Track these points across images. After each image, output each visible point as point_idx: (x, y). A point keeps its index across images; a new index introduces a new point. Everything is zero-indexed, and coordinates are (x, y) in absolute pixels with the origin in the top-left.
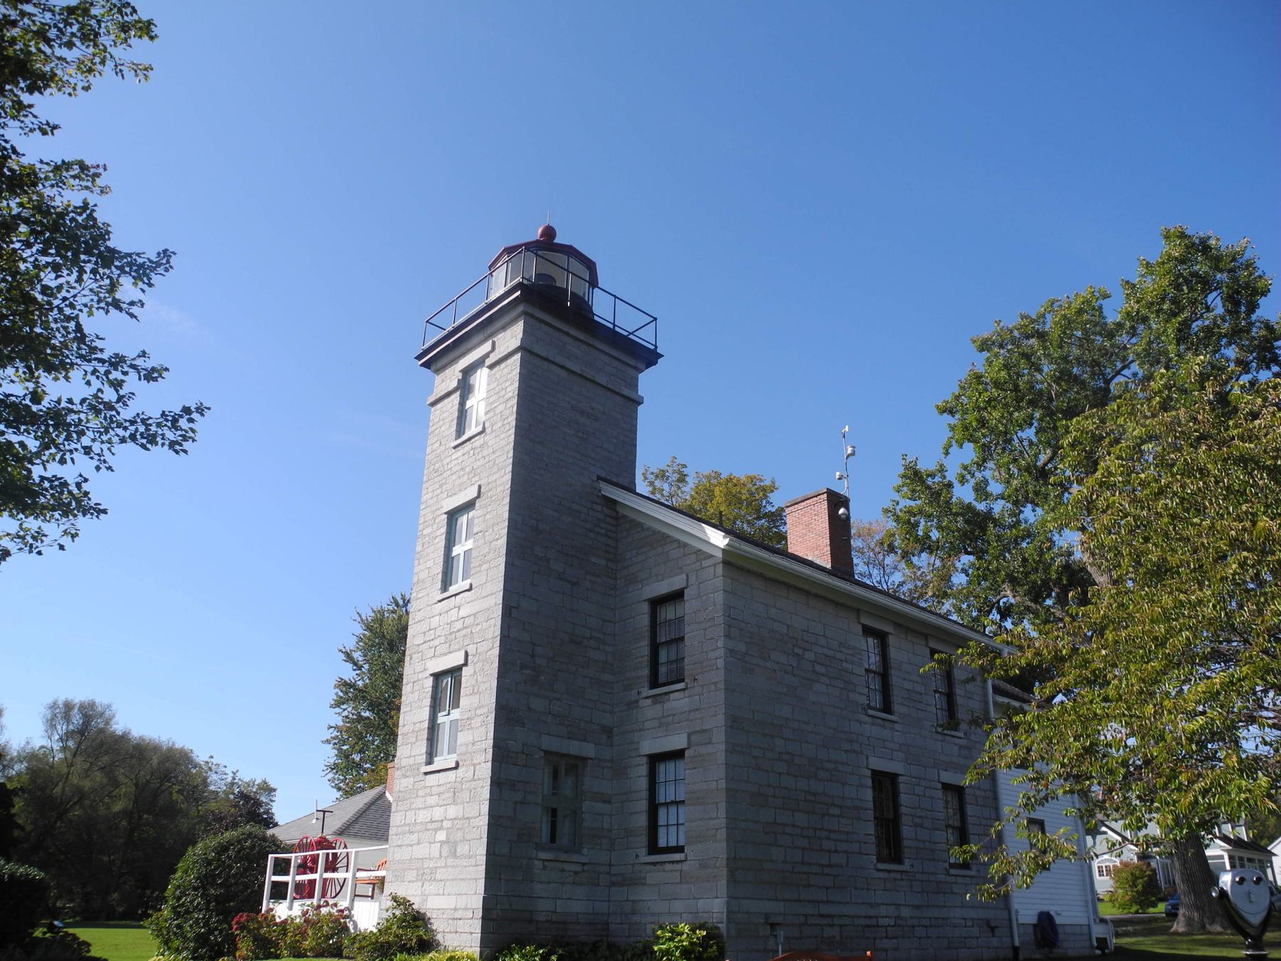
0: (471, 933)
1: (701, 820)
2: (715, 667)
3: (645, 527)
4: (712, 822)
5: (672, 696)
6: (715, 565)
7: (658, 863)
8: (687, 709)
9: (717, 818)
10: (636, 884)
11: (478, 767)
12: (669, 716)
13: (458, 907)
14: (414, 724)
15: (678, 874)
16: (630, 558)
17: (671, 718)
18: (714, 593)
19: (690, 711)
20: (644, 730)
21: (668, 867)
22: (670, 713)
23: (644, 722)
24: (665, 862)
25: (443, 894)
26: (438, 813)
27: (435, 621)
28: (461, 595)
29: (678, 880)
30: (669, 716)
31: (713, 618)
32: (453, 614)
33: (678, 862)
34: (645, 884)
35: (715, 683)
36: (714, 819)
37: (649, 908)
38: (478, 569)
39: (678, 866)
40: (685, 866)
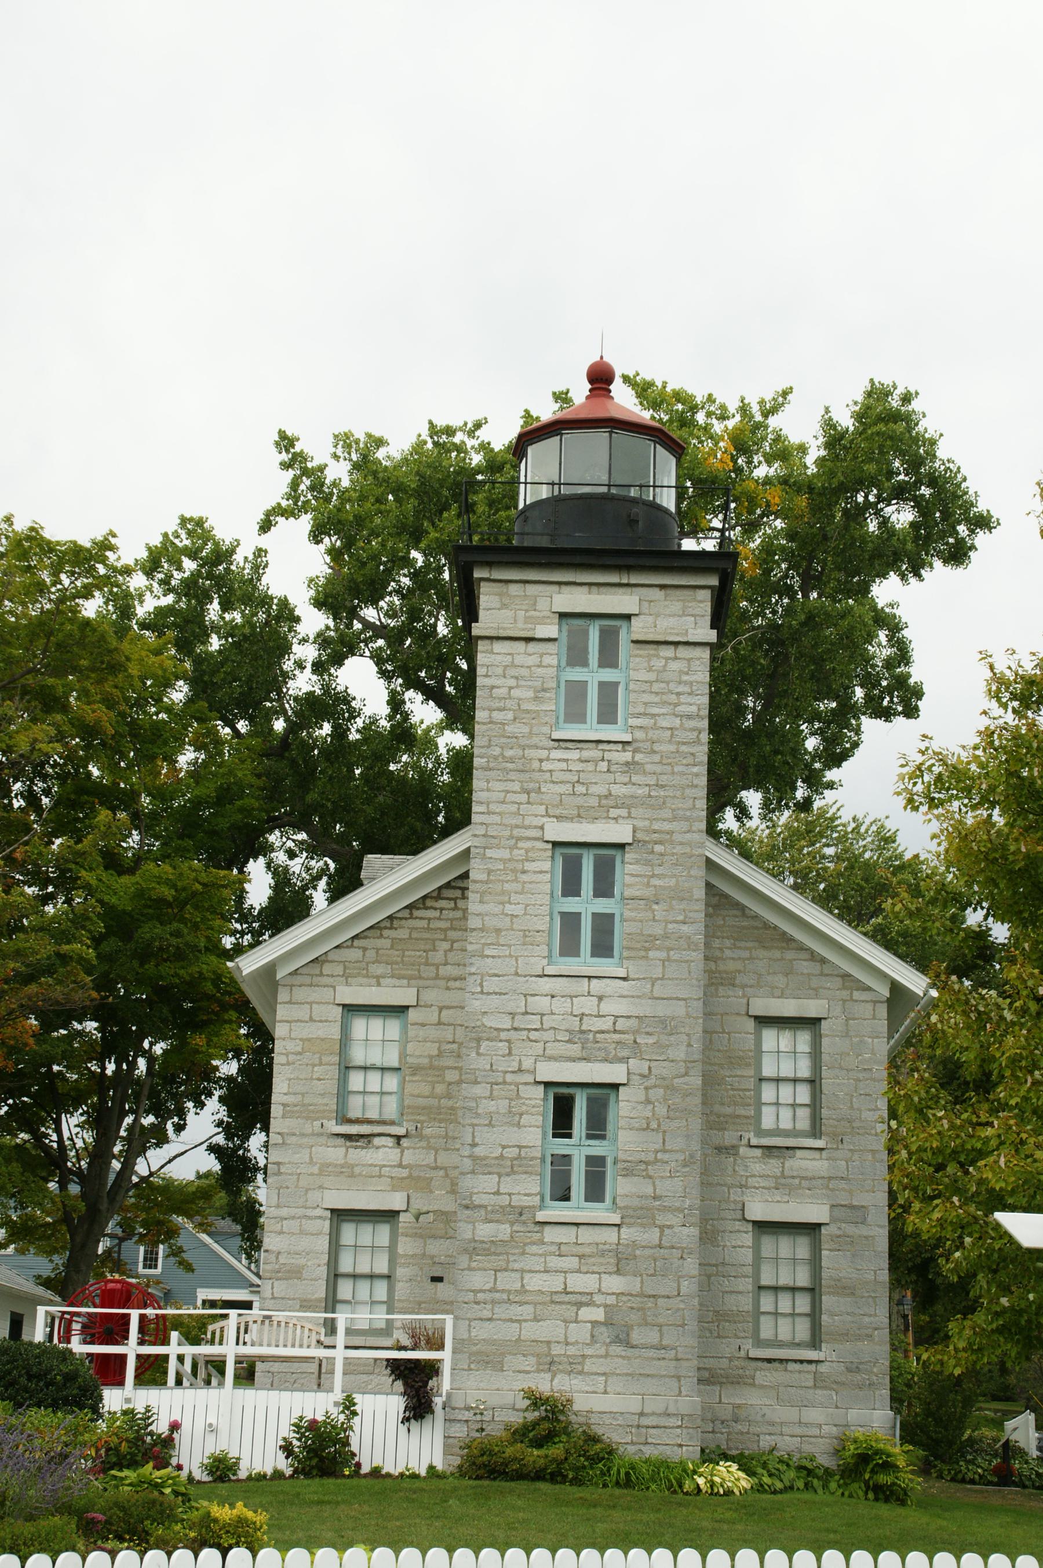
0: (681, 1446)
1: (848, 1314)
2: (873, 1132)
3: (747, 911)
4: (867, 1319)
5: (799, 1153)
6: (875, 1002)
7: (775, 1360)
8: (826, 1175)
9: (876, 1315)
10: (739, 1383)
11: (667, 1231)
12: (793, 1177)
13: (645, 1411)
14: (504, 1147)
15: (811, 1376)
16: (721, 949)
17: (797, 1181)
18: (873, 1038)
19: (830, 1178)
20: (746, 1187)
21: (791, 1366)
22: (795, 1174)
23: (747, 1177)
24: (787, 1361)
25: (605, 1392)
26: (581, 1282)
27: (542, 1003)
28: (605, 980)
29: (811, 1383)
30: (793, 1177)
31: (870, 1070)
32: (588, 1005)
33: (810, 1362)
34: (753, 1385)
35: (873, 1152)
36: (871, 1315)
37: (764, 1415)
38: (643, 953)
39: (812, 1367)
40: (823, 1368)
